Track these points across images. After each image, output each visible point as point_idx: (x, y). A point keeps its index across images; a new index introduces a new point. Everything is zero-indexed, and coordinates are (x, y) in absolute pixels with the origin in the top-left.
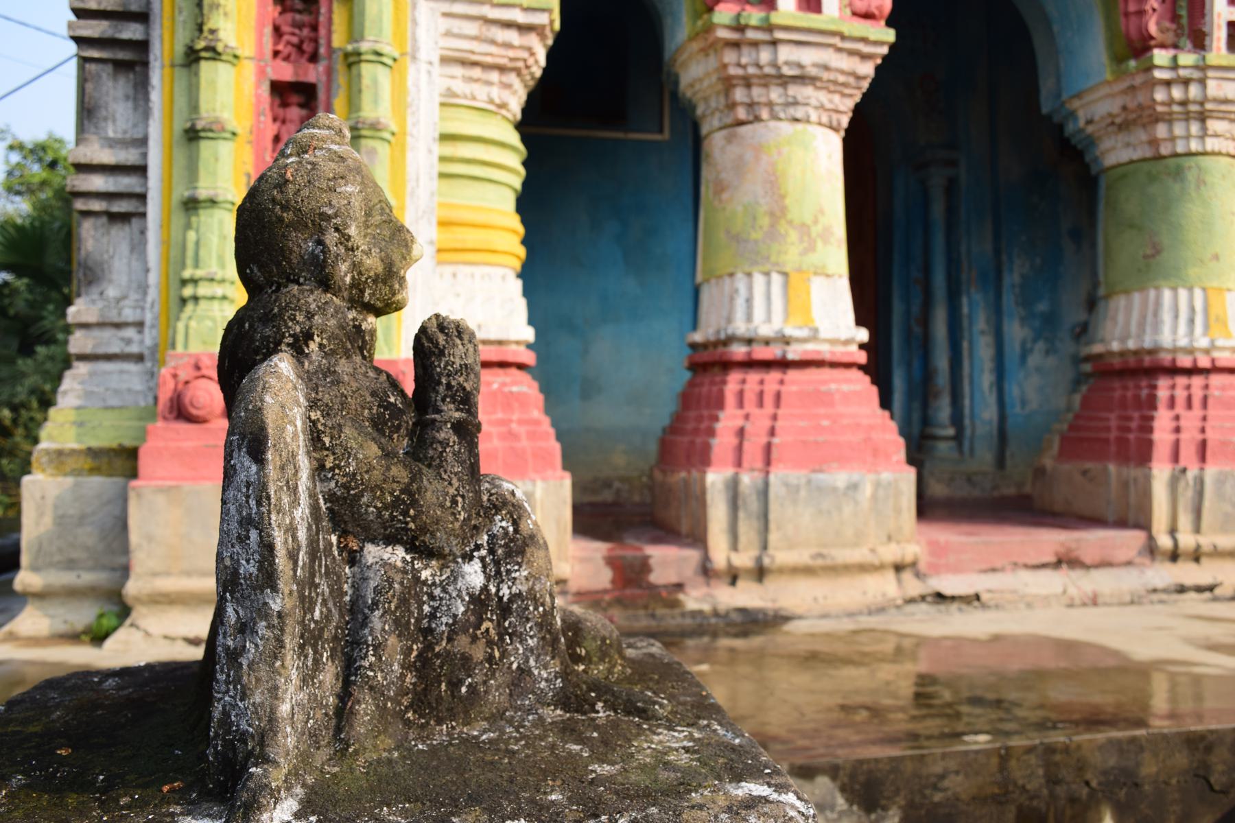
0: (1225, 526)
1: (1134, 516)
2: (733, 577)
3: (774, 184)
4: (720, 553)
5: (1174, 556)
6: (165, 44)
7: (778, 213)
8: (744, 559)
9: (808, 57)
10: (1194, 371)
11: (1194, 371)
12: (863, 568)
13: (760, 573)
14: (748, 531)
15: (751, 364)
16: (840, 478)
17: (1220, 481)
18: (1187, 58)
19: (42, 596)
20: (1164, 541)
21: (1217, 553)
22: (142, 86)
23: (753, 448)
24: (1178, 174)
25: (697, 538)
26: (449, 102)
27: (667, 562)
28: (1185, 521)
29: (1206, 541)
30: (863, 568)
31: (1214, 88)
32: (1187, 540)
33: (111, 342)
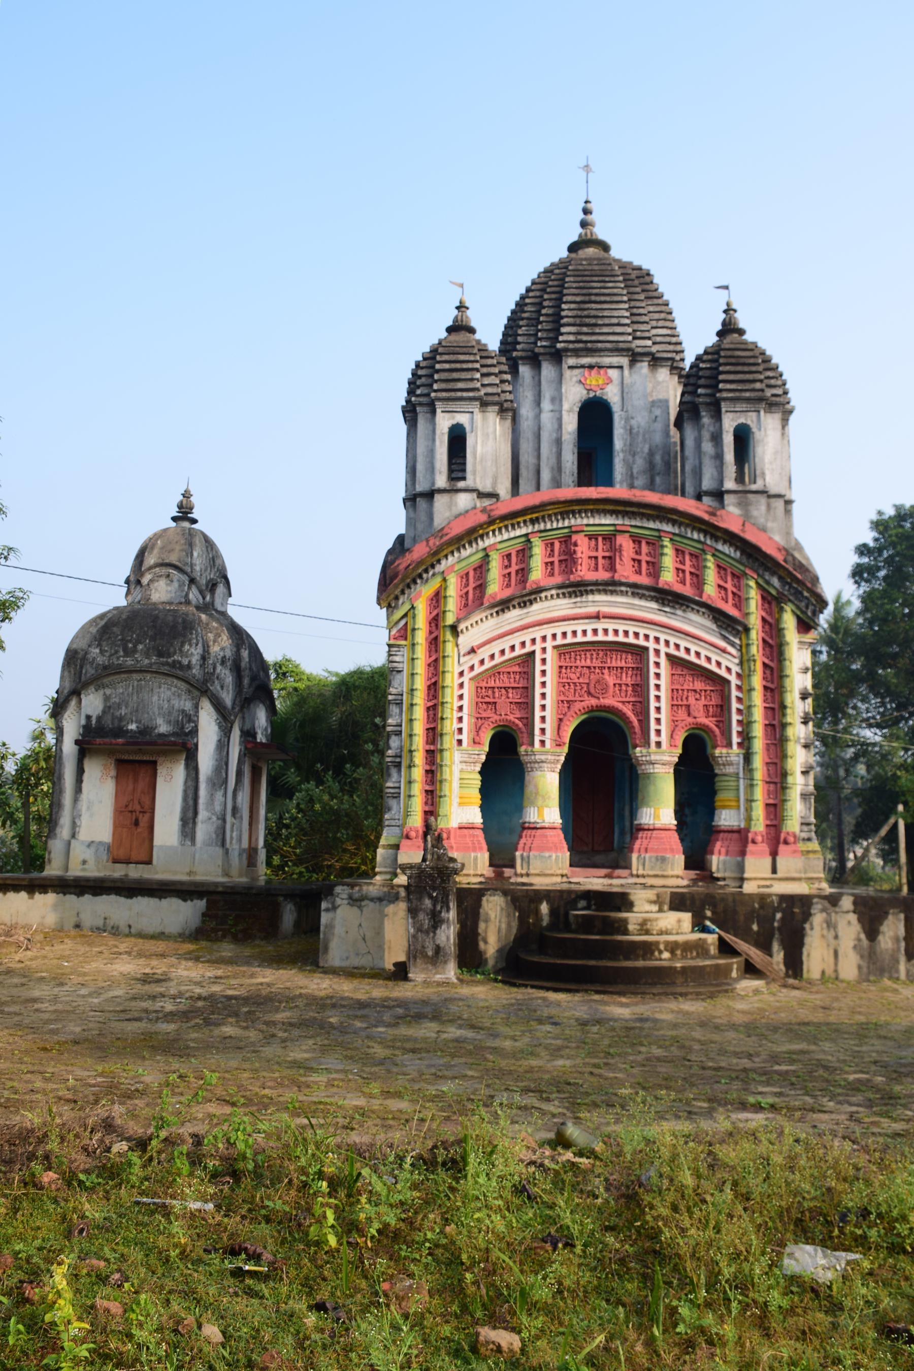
0: (652, 868)
1: (628, 866)
2: (522, 875)
3: (536, 787)
4: (519, 870)
5: (638, 876)
6: (404, 764)
7: (537, 793)
8: (524, 872)
9: (543, 757)
10: (649, 830)
11: (649, 830)
12: (552, 875)
13: (528, 875)
14: (525, 866)
15: (529, 828)
16: (547, 854)
17: (650, 858)
18: (644, 751)
19: (380, 873)
20: (635, 872)
21: (649, 876)
22: (399, 771)
23: (527, 847)
24: (648, 778)
25: (512, 865)
26: (461, 771)
27: (508, 872)
28: (641, 867)
29: (645, 873)
30: (552, 875)
31: (653, 757)
32: (641, 872)
33: (393, 823)
